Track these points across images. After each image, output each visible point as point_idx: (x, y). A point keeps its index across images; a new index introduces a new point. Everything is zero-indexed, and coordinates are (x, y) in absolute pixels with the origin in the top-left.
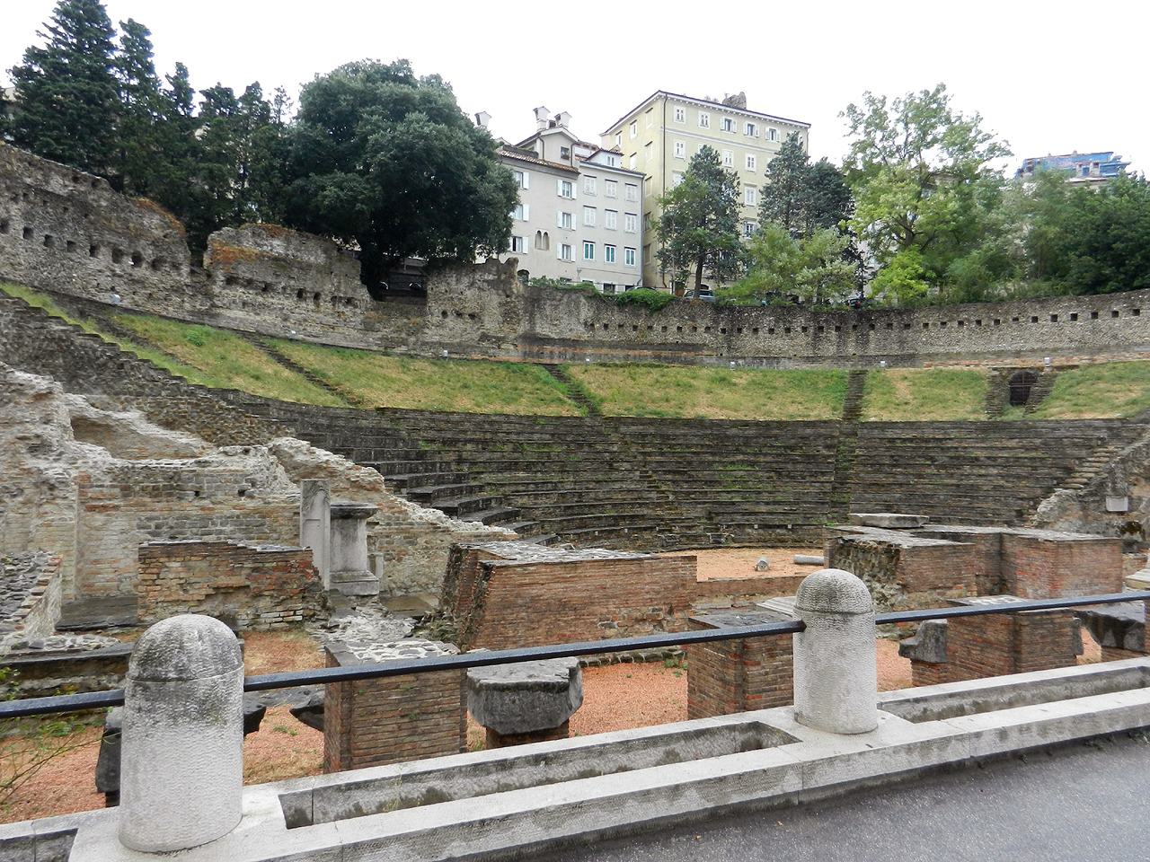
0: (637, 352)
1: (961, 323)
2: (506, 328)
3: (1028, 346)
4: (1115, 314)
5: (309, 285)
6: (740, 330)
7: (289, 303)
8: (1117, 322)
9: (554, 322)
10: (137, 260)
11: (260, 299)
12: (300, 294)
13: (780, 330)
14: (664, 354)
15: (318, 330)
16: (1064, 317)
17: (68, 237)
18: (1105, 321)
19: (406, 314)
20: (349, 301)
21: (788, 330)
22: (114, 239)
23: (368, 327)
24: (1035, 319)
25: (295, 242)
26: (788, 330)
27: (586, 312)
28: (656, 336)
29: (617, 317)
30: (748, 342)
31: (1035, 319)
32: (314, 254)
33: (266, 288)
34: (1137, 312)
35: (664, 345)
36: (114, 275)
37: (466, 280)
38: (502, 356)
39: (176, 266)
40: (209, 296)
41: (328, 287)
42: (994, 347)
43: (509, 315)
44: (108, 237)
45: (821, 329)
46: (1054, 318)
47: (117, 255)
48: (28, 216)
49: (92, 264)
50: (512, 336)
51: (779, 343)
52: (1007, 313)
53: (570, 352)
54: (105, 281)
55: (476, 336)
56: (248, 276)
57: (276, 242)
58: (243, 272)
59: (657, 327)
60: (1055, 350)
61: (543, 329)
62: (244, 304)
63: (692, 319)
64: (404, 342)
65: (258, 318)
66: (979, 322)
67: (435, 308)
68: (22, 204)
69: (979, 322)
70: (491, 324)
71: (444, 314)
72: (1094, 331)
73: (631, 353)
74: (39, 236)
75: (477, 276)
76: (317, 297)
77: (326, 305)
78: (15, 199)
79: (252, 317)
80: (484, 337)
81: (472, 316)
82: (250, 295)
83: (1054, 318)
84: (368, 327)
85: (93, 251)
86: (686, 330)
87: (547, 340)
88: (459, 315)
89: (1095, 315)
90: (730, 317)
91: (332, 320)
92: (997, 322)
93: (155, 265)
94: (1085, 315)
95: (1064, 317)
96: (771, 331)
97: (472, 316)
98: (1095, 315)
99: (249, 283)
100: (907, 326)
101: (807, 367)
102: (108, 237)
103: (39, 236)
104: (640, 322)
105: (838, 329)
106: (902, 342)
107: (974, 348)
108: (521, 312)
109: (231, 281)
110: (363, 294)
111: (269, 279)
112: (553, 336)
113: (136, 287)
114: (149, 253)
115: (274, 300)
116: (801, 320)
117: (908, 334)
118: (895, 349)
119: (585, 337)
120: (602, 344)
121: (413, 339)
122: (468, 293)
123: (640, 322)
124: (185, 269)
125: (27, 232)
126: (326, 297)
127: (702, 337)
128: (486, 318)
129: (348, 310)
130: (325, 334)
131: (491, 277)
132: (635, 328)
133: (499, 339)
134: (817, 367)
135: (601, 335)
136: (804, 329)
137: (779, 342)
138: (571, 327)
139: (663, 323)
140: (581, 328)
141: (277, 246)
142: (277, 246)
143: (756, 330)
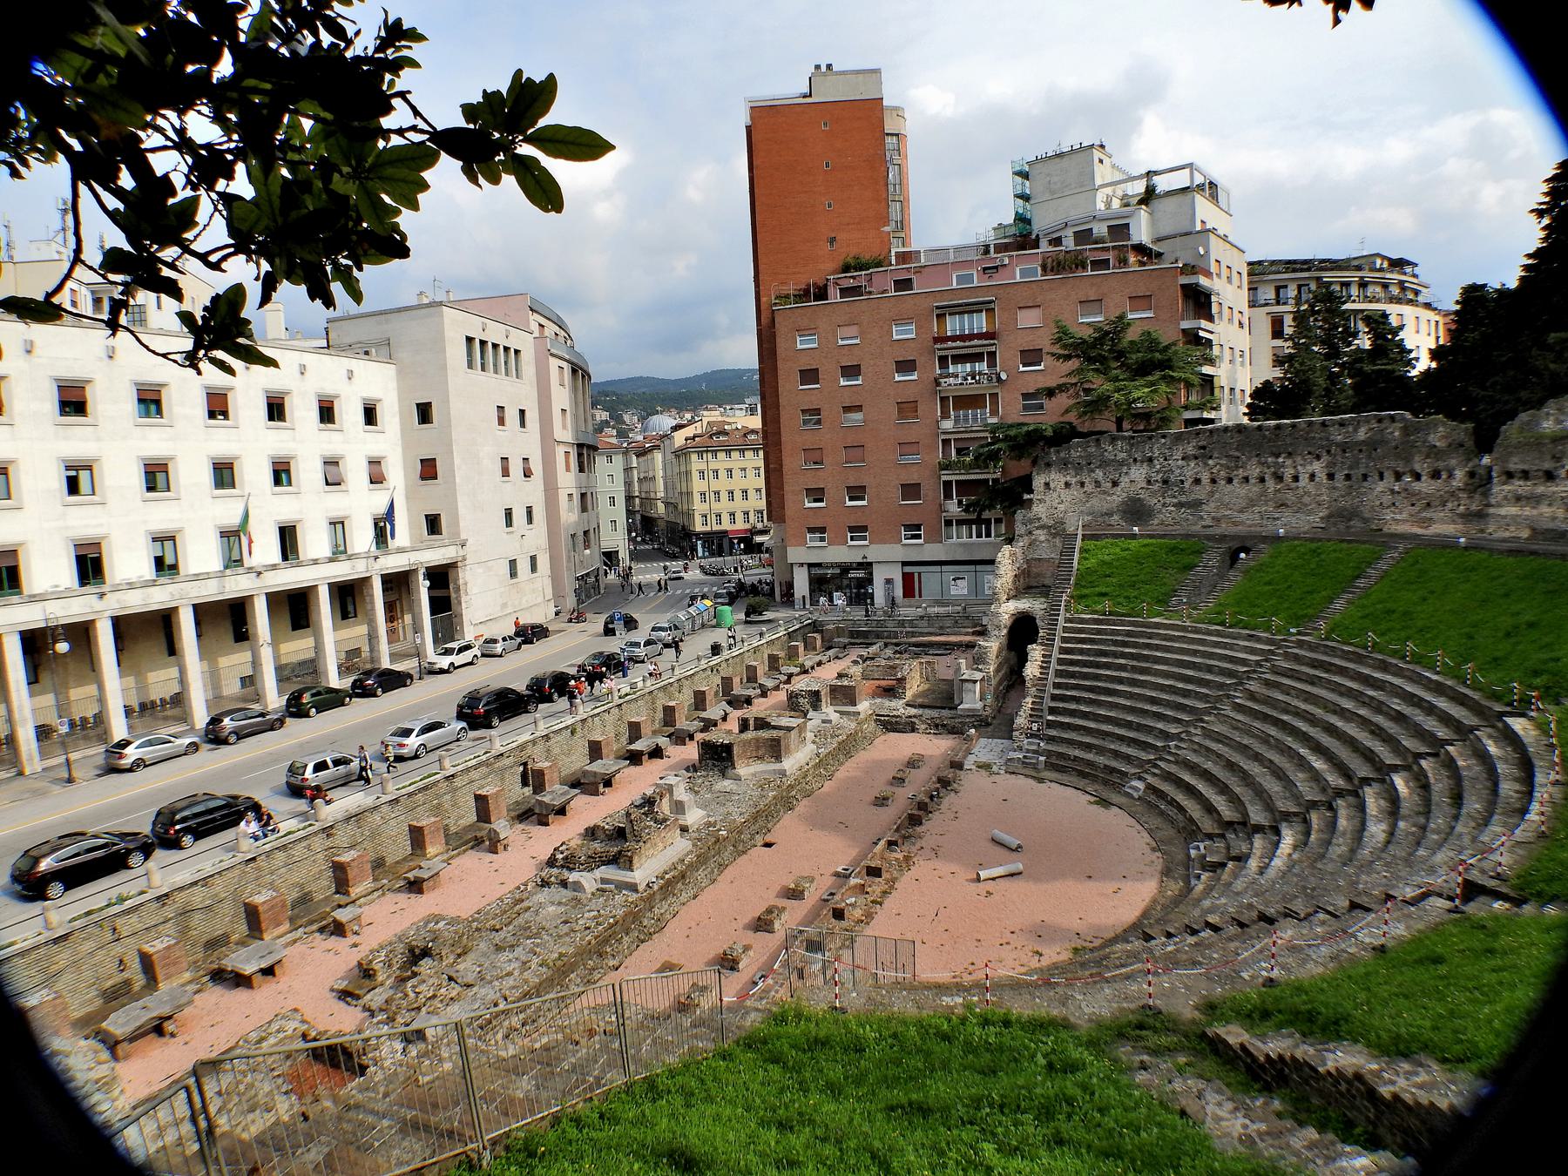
10: (1418, 477)
11: (1540, 489)
17: (1363, 471)
22: (1393, 464)
33: (1550, 476)
36: (1393, 492)
44: (1386, 464)
47: (1398, 476)
48: (1330, 465)
49: (1381, 487)
54: (1387, 499)
58: (1515, 464)
62: (1518, 499)
65: (1535, 512)
68: (1325, 458)
78: (1318, 458)
79: (1528, 511)
85: (1381, 478)
93: (1435, 475)
99: (1525, 475)
103: (1340, 476)
109: (1510, 475)
111: (1547, 465)
113: (1414, 500)
125: (1331, 476)
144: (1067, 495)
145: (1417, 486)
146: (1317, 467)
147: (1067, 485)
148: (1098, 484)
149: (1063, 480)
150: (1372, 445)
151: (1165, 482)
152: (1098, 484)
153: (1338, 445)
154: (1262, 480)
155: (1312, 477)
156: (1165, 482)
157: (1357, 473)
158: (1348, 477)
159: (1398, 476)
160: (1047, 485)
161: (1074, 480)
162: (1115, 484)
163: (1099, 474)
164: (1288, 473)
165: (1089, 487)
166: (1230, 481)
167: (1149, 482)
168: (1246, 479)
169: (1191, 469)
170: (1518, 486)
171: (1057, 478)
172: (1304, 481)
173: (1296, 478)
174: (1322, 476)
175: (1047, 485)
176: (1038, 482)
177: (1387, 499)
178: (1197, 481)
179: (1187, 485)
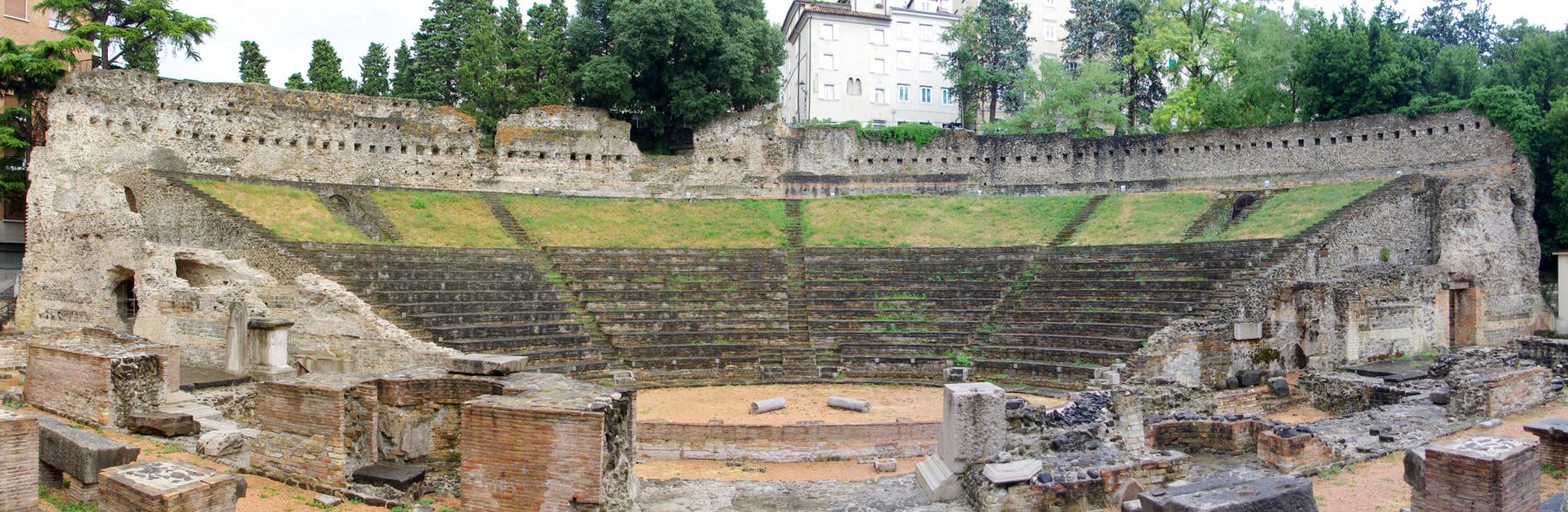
0: (900, 185)
1: (1207, 148)
2: (769, 169)
3: (1264, 171)
4: (1333, 140)
5: (579, 149)
6: (1003, 159)
7: (564, 165)
8: (1335, 148)
9: (816, 159)
10: (436, 151)
11: (537, 165)
12: (573, 157)
13: (1042, 158)
14: (927, 185)
15: (589, 184)
16: (1293, 143)
18: (1325, 147)
19: (674, 164)
20: (619, 158)
21: (1049, 157)
23: (635, 176)
24: (1270, 145)
25: (571, 115)
26: (1049, 157)
27: (850, 147)
28: (922, 169)
29: (880, 152)
30: (1012, 172)
31: (1270, 145)
32: (588, 121)
33: (542, 156)
34: (1350, 139)
35: (927, 178)
37: (731, 129)
38: (764, 194)
39: (466, 150)
40: (493, 167)
41: (597, 149)
42: (1235, 172)
43: (772, 156)
45: (1080, 155)
46: (1285, 143)
47: (420, 149)
49: (402, 158)
50: (775, 176)
51: (1040, 172)
52: (1246, 137)
53: (833, 187)
55: (739, 178)
56: (525, 148)
57: (554, 119)
58: (520, 146)
59: (922, 160)
60: (1286, 175)
61: (806, 166)
63: (955, 148)
64: (669, 188)
66: (1222, 147)
67: (700, 156)
68: (353, 130)
69: (1222, 147)
70: (755, 165)
71: (710, 160)
72: (1317, 156)
73: (895, 185)
74: (365, 147)
75: (742, 124)
76: (588, 157)
77: (596, 163)
78: (348, 127)
79: (529, 179)
80: (748, 178)
81: (737, 160)
82: (528, 163)
83: (1285, 143)
84: (635, 176)
85: (404, 149)
86: (950, 161)
87: (813, 178)
88: (725, 160)
89: (1318, 141)
90: (996, 145)
91: (601, 176)
92: (1238, 146)
93: (451, 150)
94: (1309, 141)
95: (1293, 143)
96: (1034, 159)
97: (737, 160)
98: (1318, 141)
100: (1160, 151)
101: (1066, 193)
102: (412, 138)
103: (365, 147)
104: (906, 156)
105: (1096, 155)
106: (1154, 166)
107: (1218, 173)
108: (785, 154)
109: (511, 154)
110: (632, 150)
111: (544, 149)
112: (818, 173)
114: (443, 143)
115: (549, 164)
116: (1062, 147)
117: (1159, 158)
118: (1149, 175)
119: (849, 172)
120: (863, 179)
121: (678, 185)
122: (733, 140)
123: (906, 156)
124: (473, 151)
125: (357, 146)
126: (596, 156)
127: (966, 167)
128: (751, 162)
129: (617, 166)
130: (595, 188)
131: (756, 123)
132: (900, 161)
133: (761, 179)
134: (1076, 193)
135: (866, 170)
136: (1065, 156)
137: (1041, 170)
138: (835, 163)
139: (928, 155)
140: (845, 164)
141: (555, 121)
142: (555, 121)
143: (1019, 159)
144: (91, 130)
145: (436, 159)
146: (349, 136)
147: (93, 121)
148: (126, 124)
149: (90, 113)
150: (397, 122)
151: (195, 135)
152: (126, 124)
153: (364, 119)
154: (294, 143)
155: (342, 145)
156: (195, 135)
157: (380, 148)
158: (372, 147)
159: (420, 149)
160: (70, 118)
161: (103, 117)
162: (144, 128)
163: (130, 113)
164: (321, 137)
165: (117, 128)
166: (262, 141)
167: (178, 132)
168: (277, 141)
169: (221, 126)
170: (517, 162)
171: (84, 111)
172: (334, 147)
173: (326, 146)
174: (350, 145)
175: (70, 118)
176: (58, 109)
177: (411, 169)
178: (228, 138)
179: (219, 140)
